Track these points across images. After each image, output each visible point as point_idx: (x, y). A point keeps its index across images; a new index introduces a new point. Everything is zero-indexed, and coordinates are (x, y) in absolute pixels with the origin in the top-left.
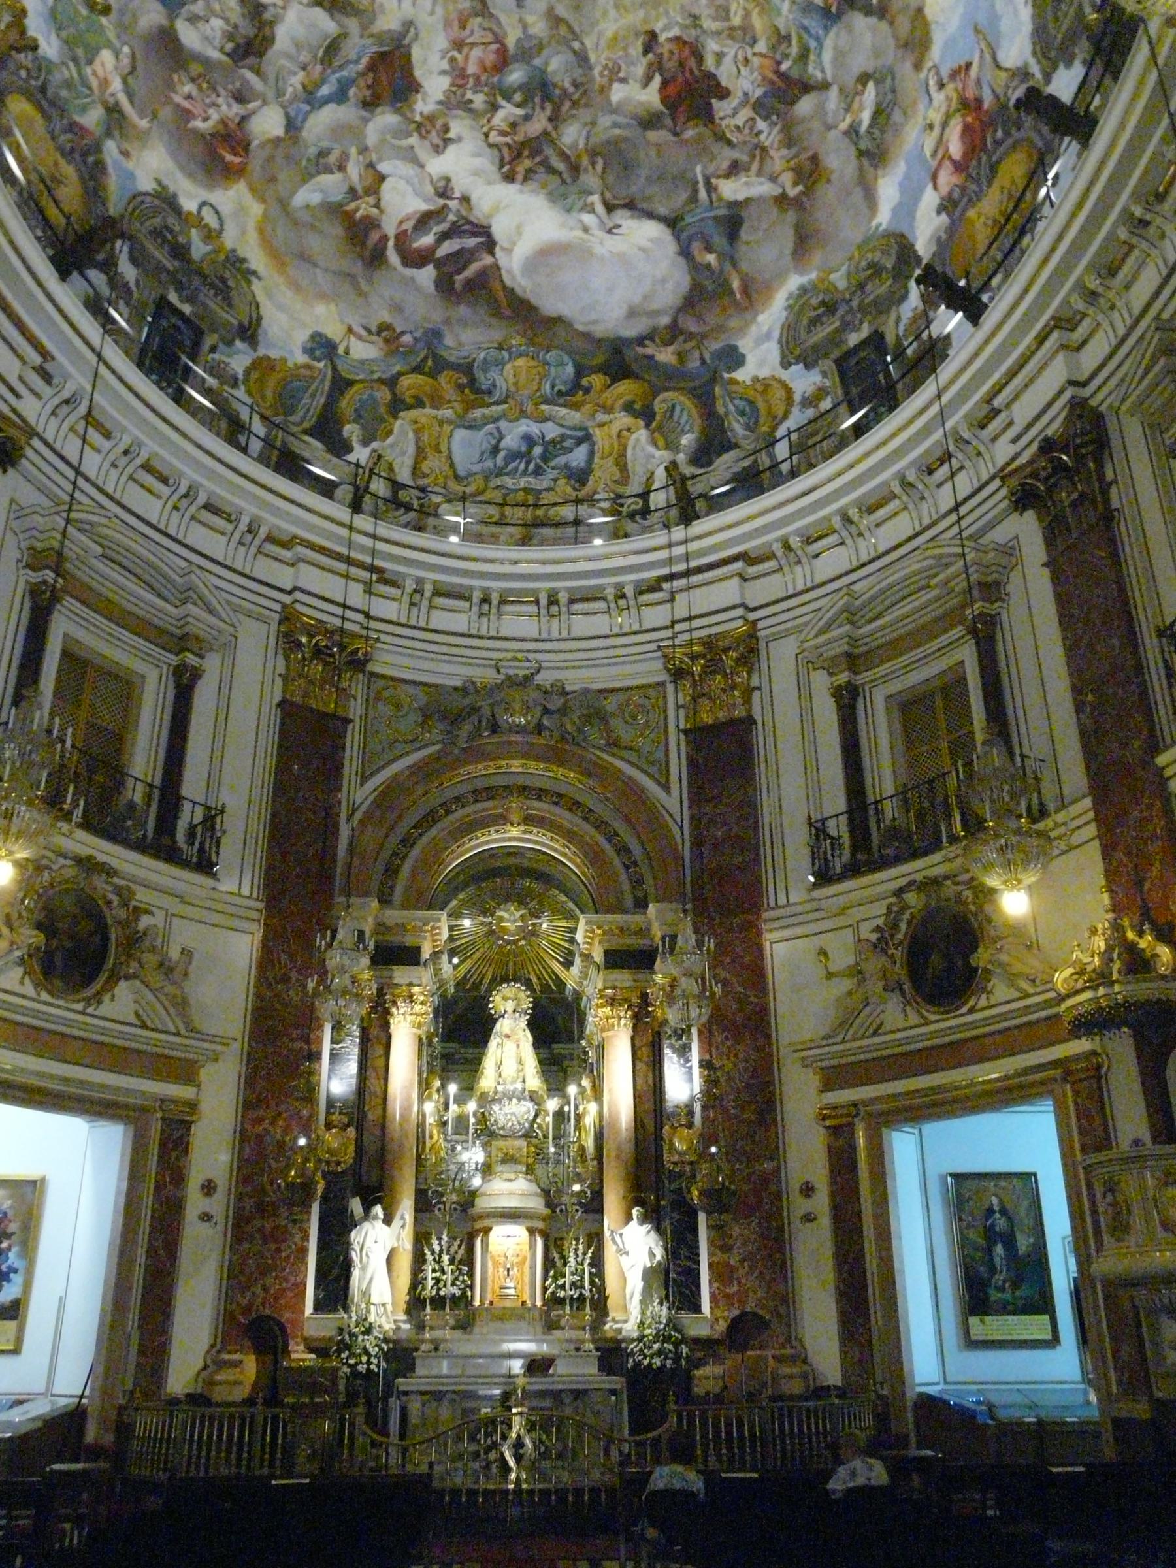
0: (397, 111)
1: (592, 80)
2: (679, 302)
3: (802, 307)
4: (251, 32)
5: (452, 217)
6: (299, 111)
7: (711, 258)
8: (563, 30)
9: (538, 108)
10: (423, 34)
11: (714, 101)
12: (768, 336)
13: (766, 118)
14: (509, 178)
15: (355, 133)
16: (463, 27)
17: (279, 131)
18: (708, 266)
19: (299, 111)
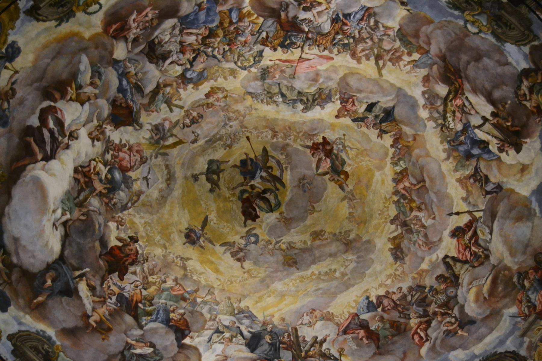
0: (108, 117)
1: (117, 214)
2: (24, 267)
3: (40, 340)
4: (158, 53)
5: (60, 138)
6: (120, 67)
7: (49, 282)
8: (135, 198)
9: (105, 186)
10: (135, 133)
11: (117, 273)
12: (20, 324)
13: (117, 299)
14: (76, 170)
15: (103, 94)
16: (137, 151)
17: (115, 56)
18: (46, 282)
19: (120, 67)
